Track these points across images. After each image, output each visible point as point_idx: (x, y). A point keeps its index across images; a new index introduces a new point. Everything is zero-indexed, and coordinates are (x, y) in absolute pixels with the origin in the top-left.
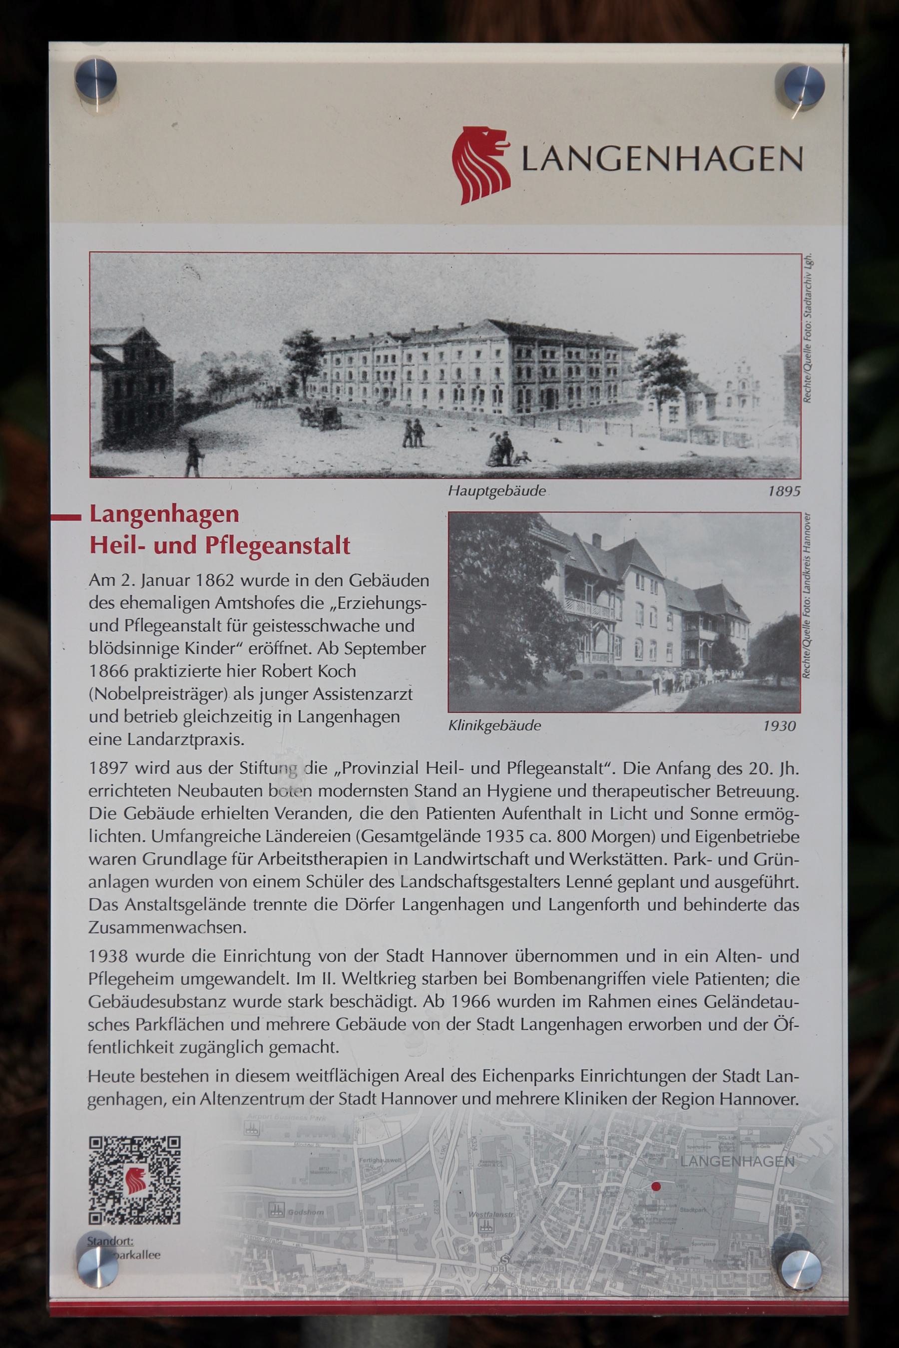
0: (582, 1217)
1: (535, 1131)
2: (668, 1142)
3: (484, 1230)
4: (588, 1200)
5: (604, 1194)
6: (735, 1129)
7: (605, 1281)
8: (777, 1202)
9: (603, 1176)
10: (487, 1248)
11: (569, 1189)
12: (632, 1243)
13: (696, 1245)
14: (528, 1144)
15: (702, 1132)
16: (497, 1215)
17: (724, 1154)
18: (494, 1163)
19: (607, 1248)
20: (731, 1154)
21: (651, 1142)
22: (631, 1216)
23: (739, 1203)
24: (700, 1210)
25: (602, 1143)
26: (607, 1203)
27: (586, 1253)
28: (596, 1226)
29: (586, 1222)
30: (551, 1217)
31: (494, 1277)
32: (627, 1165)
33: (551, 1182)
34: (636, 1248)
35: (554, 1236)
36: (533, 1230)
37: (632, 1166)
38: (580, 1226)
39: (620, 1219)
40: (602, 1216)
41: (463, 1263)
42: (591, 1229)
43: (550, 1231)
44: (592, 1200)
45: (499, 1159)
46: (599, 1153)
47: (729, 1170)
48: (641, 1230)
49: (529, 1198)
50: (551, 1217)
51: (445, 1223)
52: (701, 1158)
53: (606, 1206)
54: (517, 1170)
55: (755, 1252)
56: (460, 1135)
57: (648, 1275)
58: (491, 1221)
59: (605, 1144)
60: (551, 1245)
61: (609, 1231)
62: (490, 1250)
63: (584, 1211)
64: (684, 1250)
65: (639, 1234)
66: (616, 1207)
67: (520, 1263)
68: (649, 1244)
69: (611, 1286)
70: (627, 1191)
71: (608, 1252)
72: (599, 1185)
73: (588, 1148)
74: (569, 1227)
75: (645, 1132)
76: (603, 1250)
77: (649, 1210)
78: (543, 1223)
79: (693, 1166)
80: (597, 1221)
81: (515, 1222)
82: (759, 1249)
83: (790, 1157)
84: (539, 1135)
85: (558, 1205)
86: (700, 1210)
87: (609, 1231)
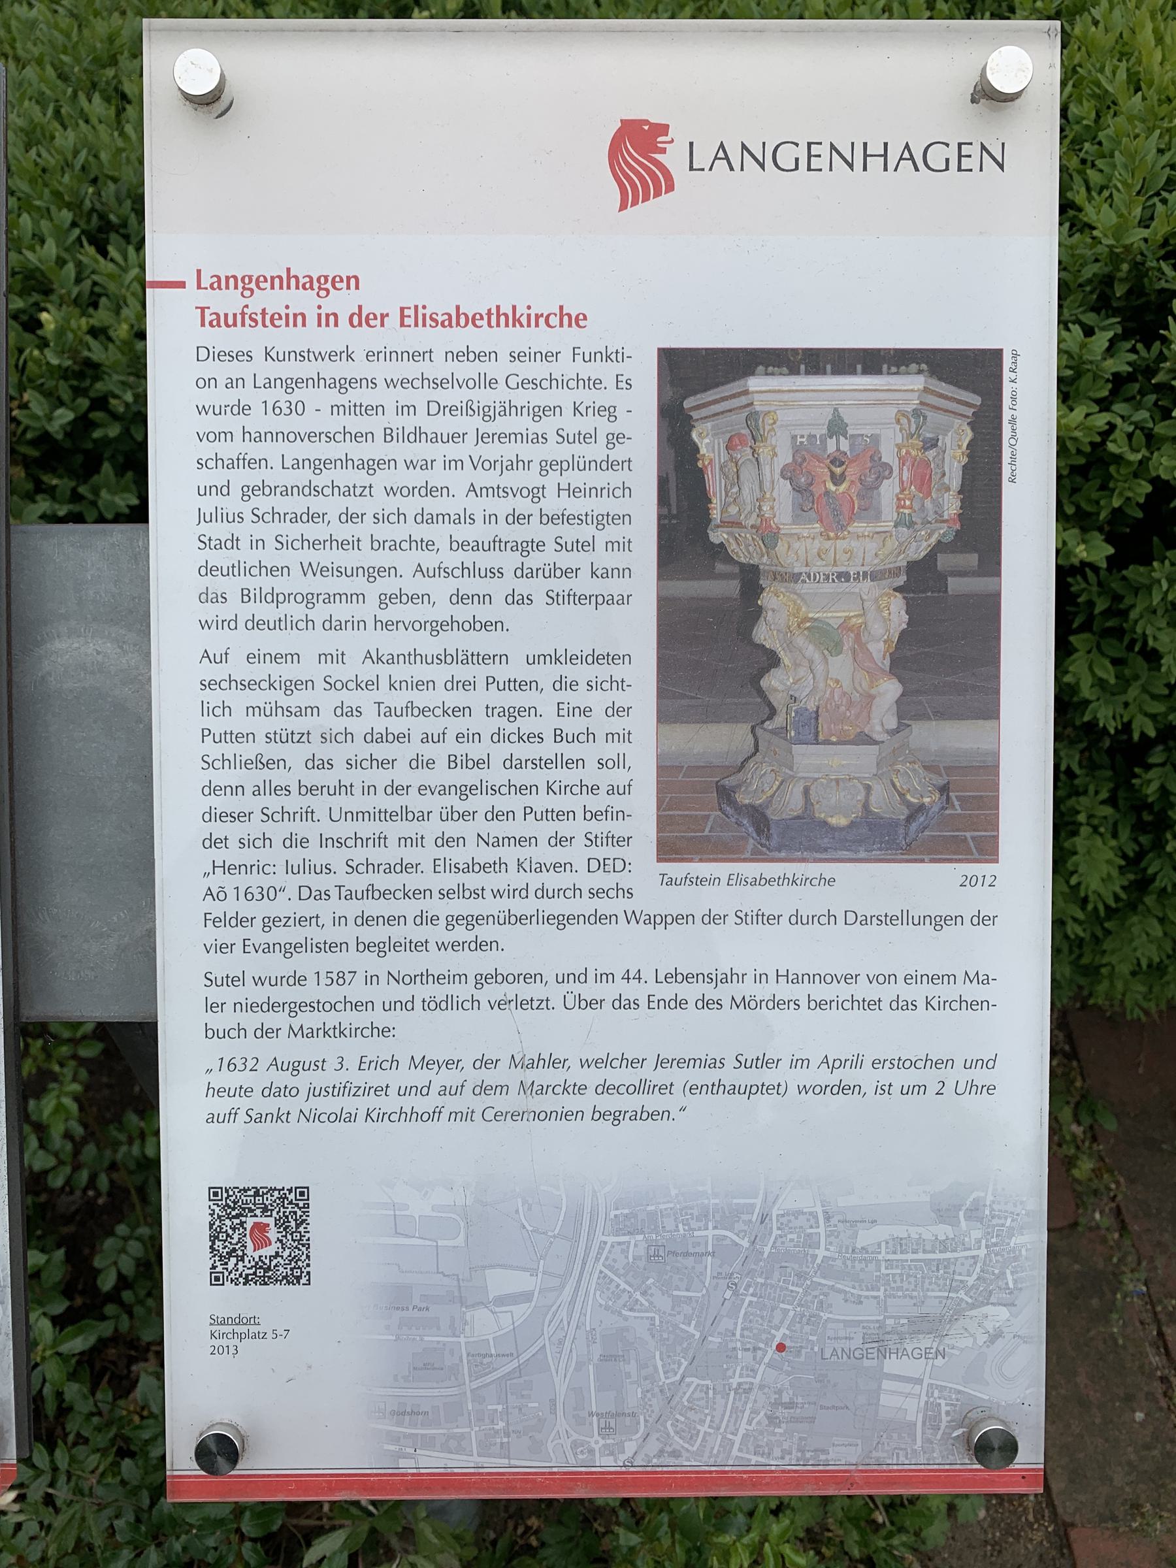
0: (713, 1417)
1: (661, 1322)
4: (719, 1397)
5: (736, 1390)
12: (767, 1445)
14: (653, 1337)
15: (844, 1321)
16: (618, 1415)
18: (614, 1358)
19: (740, 1450)
21: (787, 1332)
25: (734, 1335)
26: (740, 1400)
27: (717, 1456)
28: (727, 1426)
29: (717, 1420)
30: (678, 1416)
33: (678, 1377)
37: (766, 1360)
40: (734, 1416)
42: (722, 1430)
43: (677, 1432)
45: (621, 1353)
46: (731, 1345)
50: (678, 1416)
53: (739, 1404)
60: (678, 1448)
61: (742, 1432)
62: (612, 1454)
65: (775, 1434)
66: (749, 1405)
71: (740, 1454)
74: (699, 1427)
76: (735, 1452)
78: (669, 1423)
79: (834, 1358)
80: (729, 1421)
81: (638, 1423)
87: (742, 1432)
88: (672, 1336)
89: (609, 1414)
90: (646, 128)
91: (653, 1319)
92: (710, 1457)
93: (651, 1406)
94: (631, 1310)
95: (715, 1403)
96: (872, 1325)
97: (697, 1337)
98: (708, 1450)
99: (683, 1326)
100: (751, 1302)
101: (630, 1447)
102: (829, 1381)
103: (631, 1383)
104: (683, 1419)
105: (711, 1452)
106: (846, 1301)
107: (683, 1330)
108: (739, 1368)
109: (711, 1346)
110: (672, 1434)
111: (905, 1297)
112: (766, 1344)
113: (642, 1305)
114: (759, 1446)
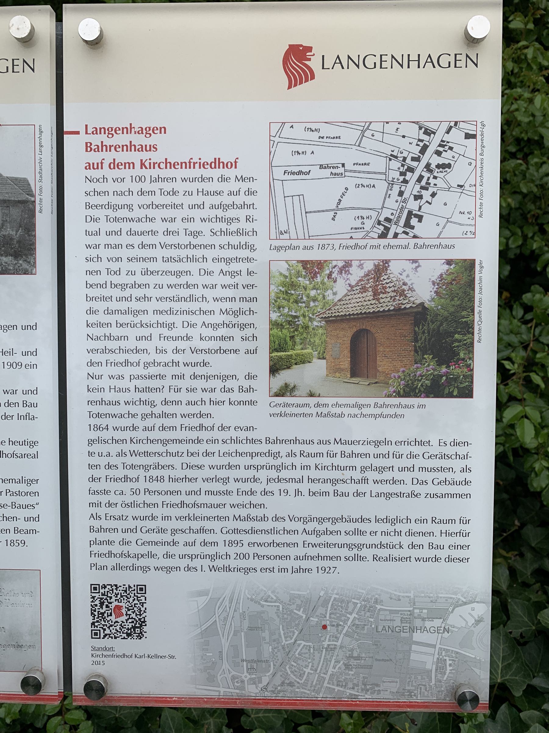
0: (313, 664)
1: (283, 609)
2: (368, 617)
3: (250, 670)
4: (316, 652)
6: (412, 609)
8: (438, 656)
9: (326, 638)
10: (253, 682)
11: (304, 645)
13: (385, 682)
14: (279, 617)
15: (390, 610)
17: (403, 625)
18: (257, 628)
19: (328, 683)
20: (408, 625)
21: (357, 616)
22: (343, 663)
23: (413, 656)
24: (388, 660)
25: (325, 617)
30: (293, 663)
33: (293, 641)
34: (346, 684)
36: (281, 671)
37: (344, 632)
39: (336, 665)
40: (325, 663)
42: (318, 672)
44: (319, 653)
47: (407, 635)
48: (350, 672)
49: (279, 651)
50: (293, 663)
51: (226, 666)
52: (389, 627)
53: (328, 657)
55: (423, 687)
56: (235, 611)
58: (255, 665)
59: (328, 618)
61: (330, 673)
62: (254, 683)
63: (314, 659)
64: (378, 685)
66: (334, 658)
70: (341, 647)
71: (328, 686)
72: (324, 643)
73: (317, 620)
74: (305, 669)
76: (326, 684)
77: (355, 660)
78: (288, 666)
79: (384, 632)
80: (322, 666)
81: (270, 666)
82: (425, 685)
83: (447, 627)
85: (297, 656)
86: (388, 660)
87: (330, 673)
89: (252, 661)
90: (301, 48)
91: (278, 606)
92: (311, 687)
93: (277, 656)
94: (266, 601)
95: (314, 656)
96: (406, 613)
97: (304, 617)
98: (310, 683)
100: (335, 598)
101: (265, 680)
102: (381, 645)
104: (295, 664)
106: (391, 598)
108: (328, 636)
109: (312, 623)
111: (425, 597)
112: (344, 623)
113: (272, 598)
114: (339, 681)
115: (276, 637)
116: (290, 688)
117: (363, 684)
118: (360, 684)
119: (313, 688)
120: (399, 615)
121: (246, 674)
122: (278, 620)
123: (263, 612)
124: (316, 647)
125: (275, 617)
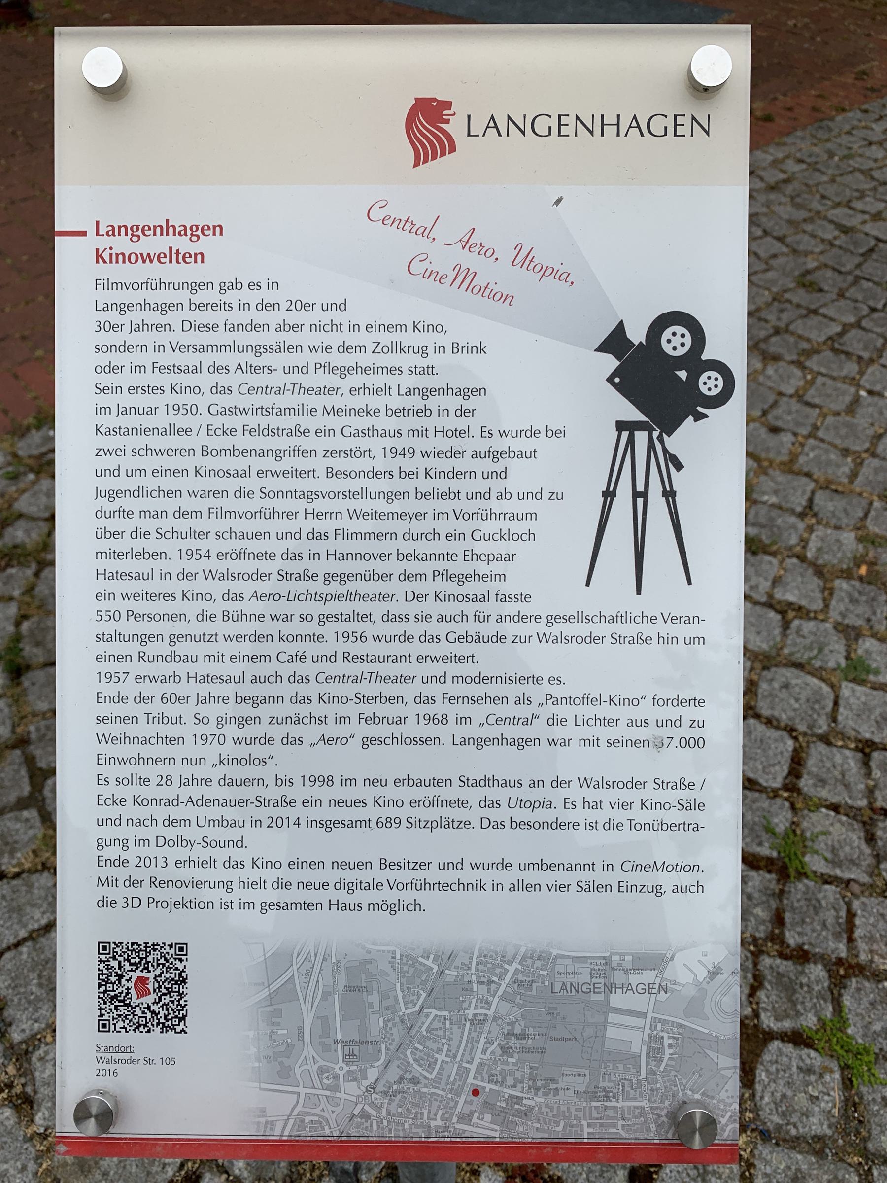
0: (450, 1046)
1: (401, 955)
3: (349, 1058)
4: (455, 1027)
6: (607, 954)
7: (472, 1113)
10: (352, 1077)
12: (501, 1073)
16: (361, 1043)
17: (595, 980)
18: (360, 989)
21: (520, 967)
24: (570, 1039)
25: (469, 968)
27: (453, 1084)
28: (463, 1055)
29: (454, 1051)
30: (417, 1045)
31: (359, 1107)
32: (496, 992)
33: (417, 1008)
34: (504, 1079)
35: (420, 1066)
36: (399, 1058)
37: (500, 993)
38: (447, 1056)
40: (469, 1045)
41: (328, 1093)
42: (458, 1059)
43: (415, 1060)
46: (466, 979)
47: (600, 997)
48: (510, 1060)
49: (394, 1025)
50: (417, 1045)
53: (473, 1034)
54: (383, 996)
56: (324, 959)
57: (517, 1106)
59: (473, 970)
60: (417, 1075)
61: (477, 1060)
62: (355, 1080)
63: (451, 1039)
64: (554, 1081)
65: (508, 1063)
67: (385, 1093)
68: (518, 1075)
69: (478, 1118)
70: (495, 1019)
74: (436, 1056)
75: (514, 958)
76: (470, 1080)
78: (409, 1051)
81: (380, 1051)
84: (405, 960)
86: (570, 1039)
87: (477, 1060)
88: (412, 970)
89: (353, 1042)
91: (394, 952)
92: (447, 1084)
96: (599, 962)
97: (435, 970)
98: (445, 1077)
99: (421, 959)
101: (373, 1074)
102: (558, 1014)
103: (374, 1013)
104: (421, 1048)
105: (448, 1080)
107: (421, 963)
108: (474, 1001)
110: (412, 1062)
112: (500, 978)
114: (492, 1075)
115: (391, 1002)
116: (411, 1086)
117: (530, 1079)
118: (527, 1077)
119: (449, 1087)
120: (588, 965)
121: (341, 1064)
122: (393, 975)
123: (370, 962)
124: (455, 1019)
125: (390, 970)
